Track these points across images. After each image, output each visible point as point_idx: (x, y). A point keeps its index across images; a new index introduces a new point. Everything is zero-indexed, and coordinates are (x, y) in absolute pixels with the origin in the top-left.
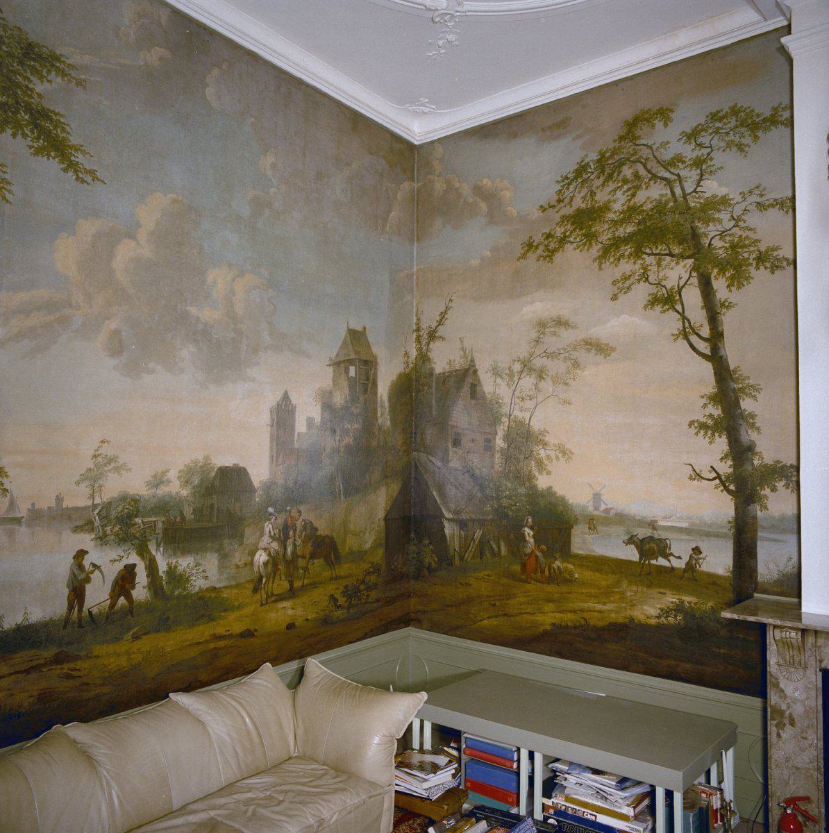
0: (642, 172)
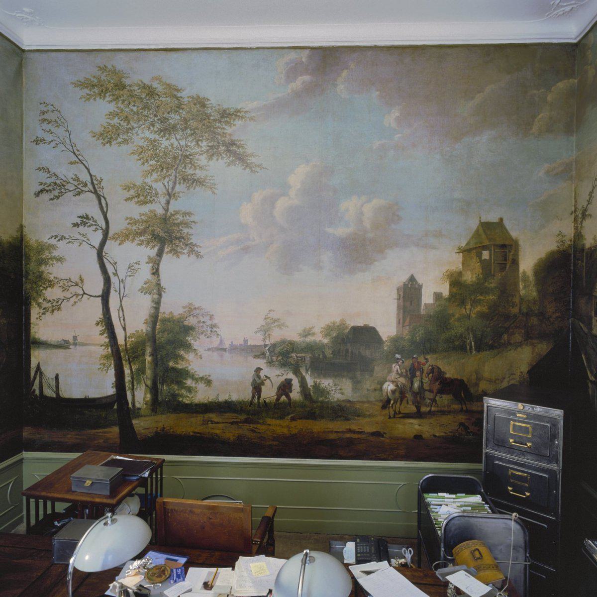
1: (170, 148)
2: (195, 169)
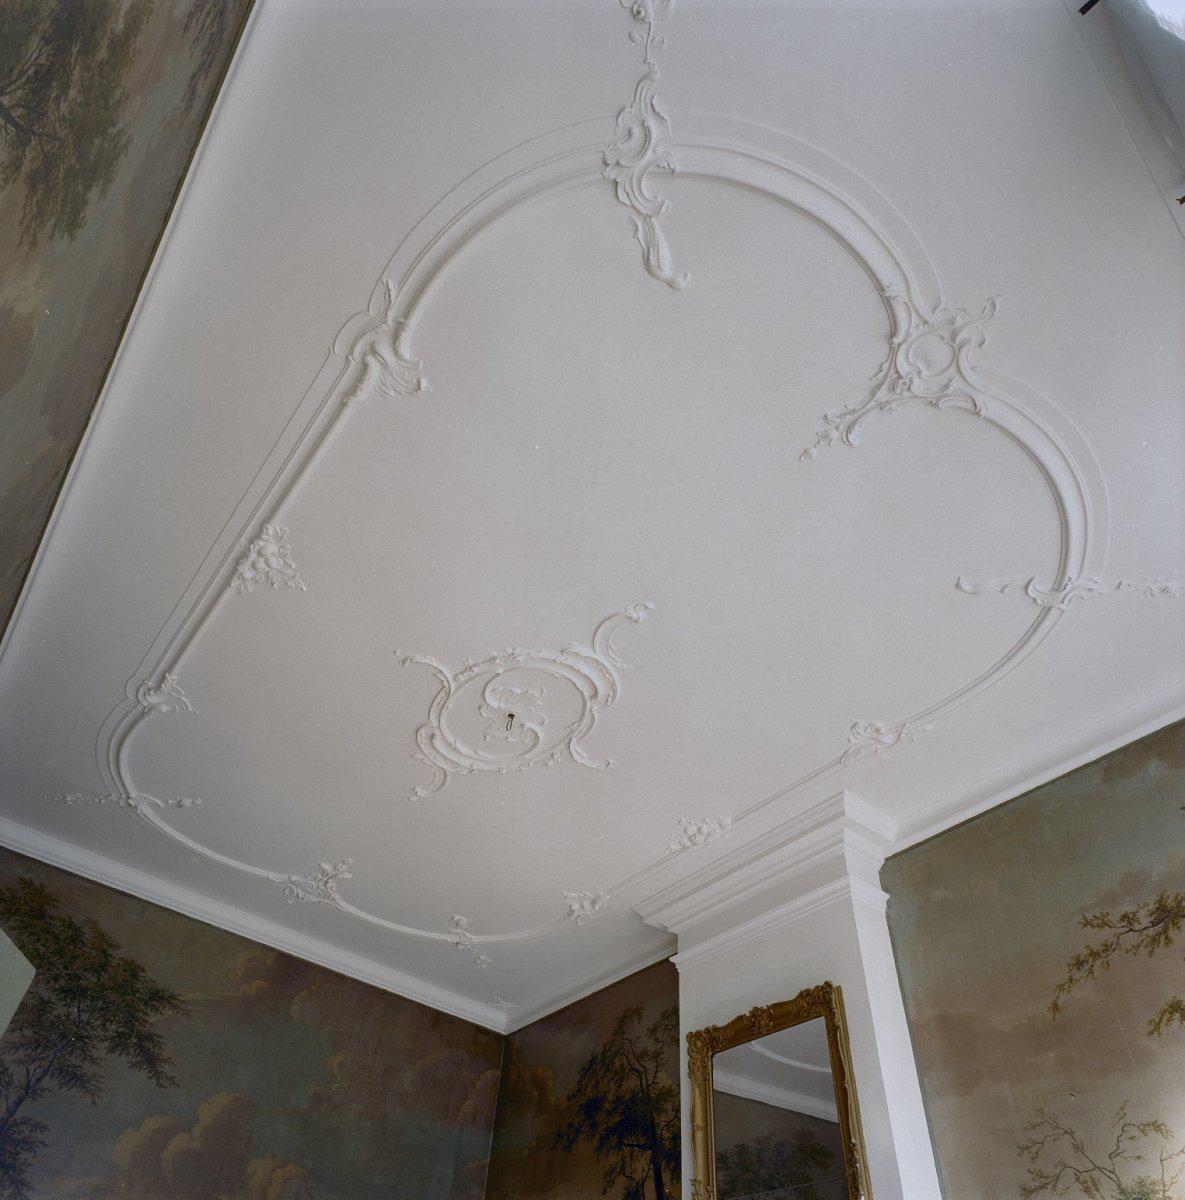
1: (63, 1018)
2: (84, 1060)
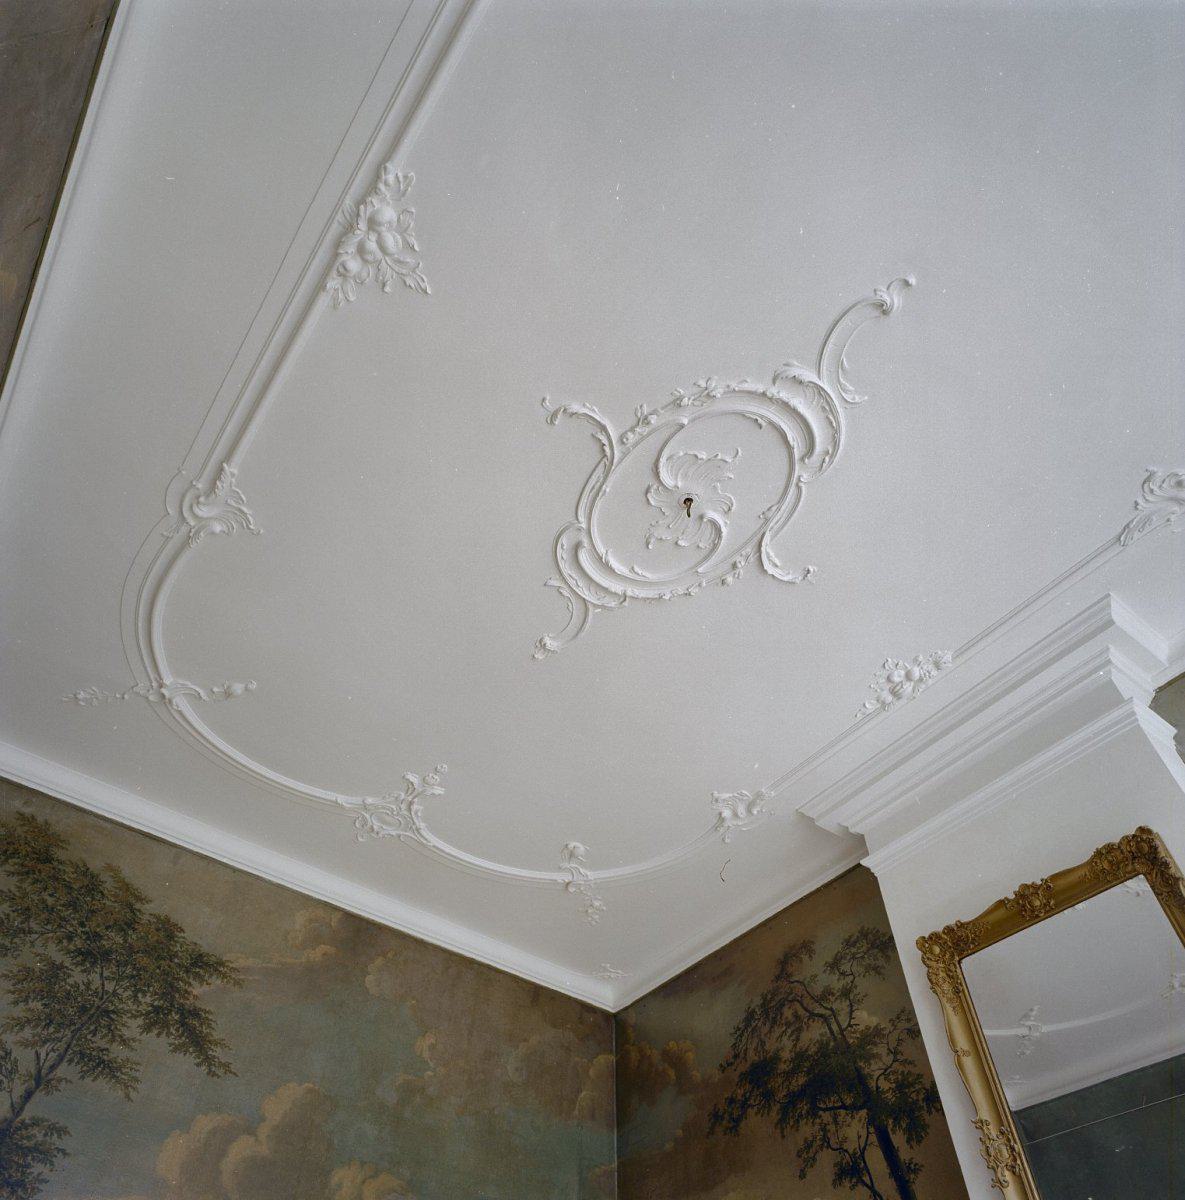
0: (801, 1012)
1: (82, 987)
2: (113, 1040)
